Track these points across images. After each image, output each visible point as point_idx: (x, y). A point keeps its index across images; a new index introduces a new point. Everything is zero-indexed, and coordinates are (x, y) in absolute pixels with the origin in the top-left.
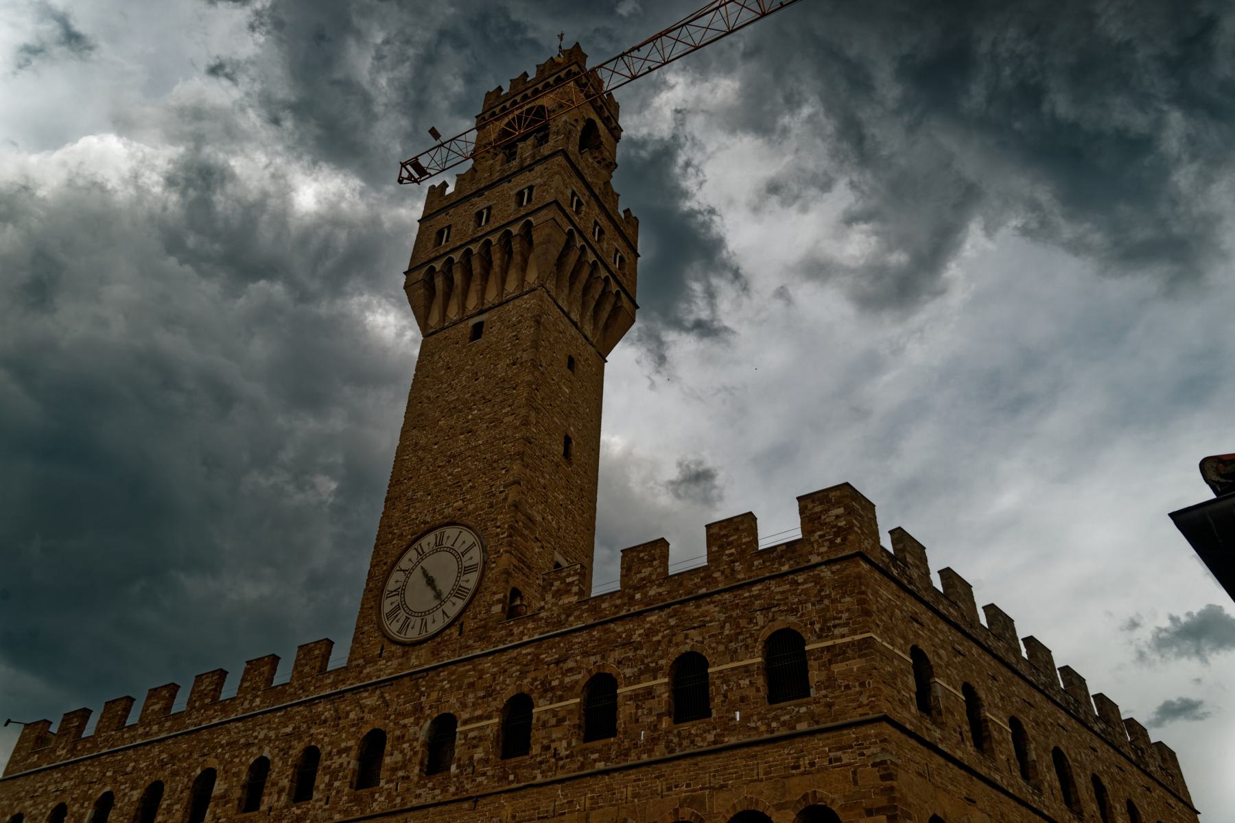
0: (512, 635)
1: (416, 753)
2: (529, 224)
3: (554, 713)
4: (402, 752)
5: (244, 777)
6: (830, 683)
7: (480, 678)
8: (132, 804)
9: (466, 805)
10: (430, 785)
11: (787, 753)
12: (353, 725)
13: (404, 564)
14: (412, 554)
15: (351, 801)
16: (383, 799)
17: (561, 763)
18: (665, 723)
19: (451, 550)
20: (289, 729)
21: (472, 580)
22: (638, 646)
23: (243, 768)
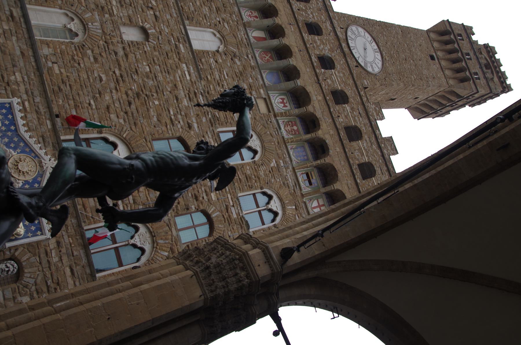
1: (321, 51)
2: (469, 80)
13: (367, 35)
14: (370, 38)
18: (357, 162)
21: (370, 69)
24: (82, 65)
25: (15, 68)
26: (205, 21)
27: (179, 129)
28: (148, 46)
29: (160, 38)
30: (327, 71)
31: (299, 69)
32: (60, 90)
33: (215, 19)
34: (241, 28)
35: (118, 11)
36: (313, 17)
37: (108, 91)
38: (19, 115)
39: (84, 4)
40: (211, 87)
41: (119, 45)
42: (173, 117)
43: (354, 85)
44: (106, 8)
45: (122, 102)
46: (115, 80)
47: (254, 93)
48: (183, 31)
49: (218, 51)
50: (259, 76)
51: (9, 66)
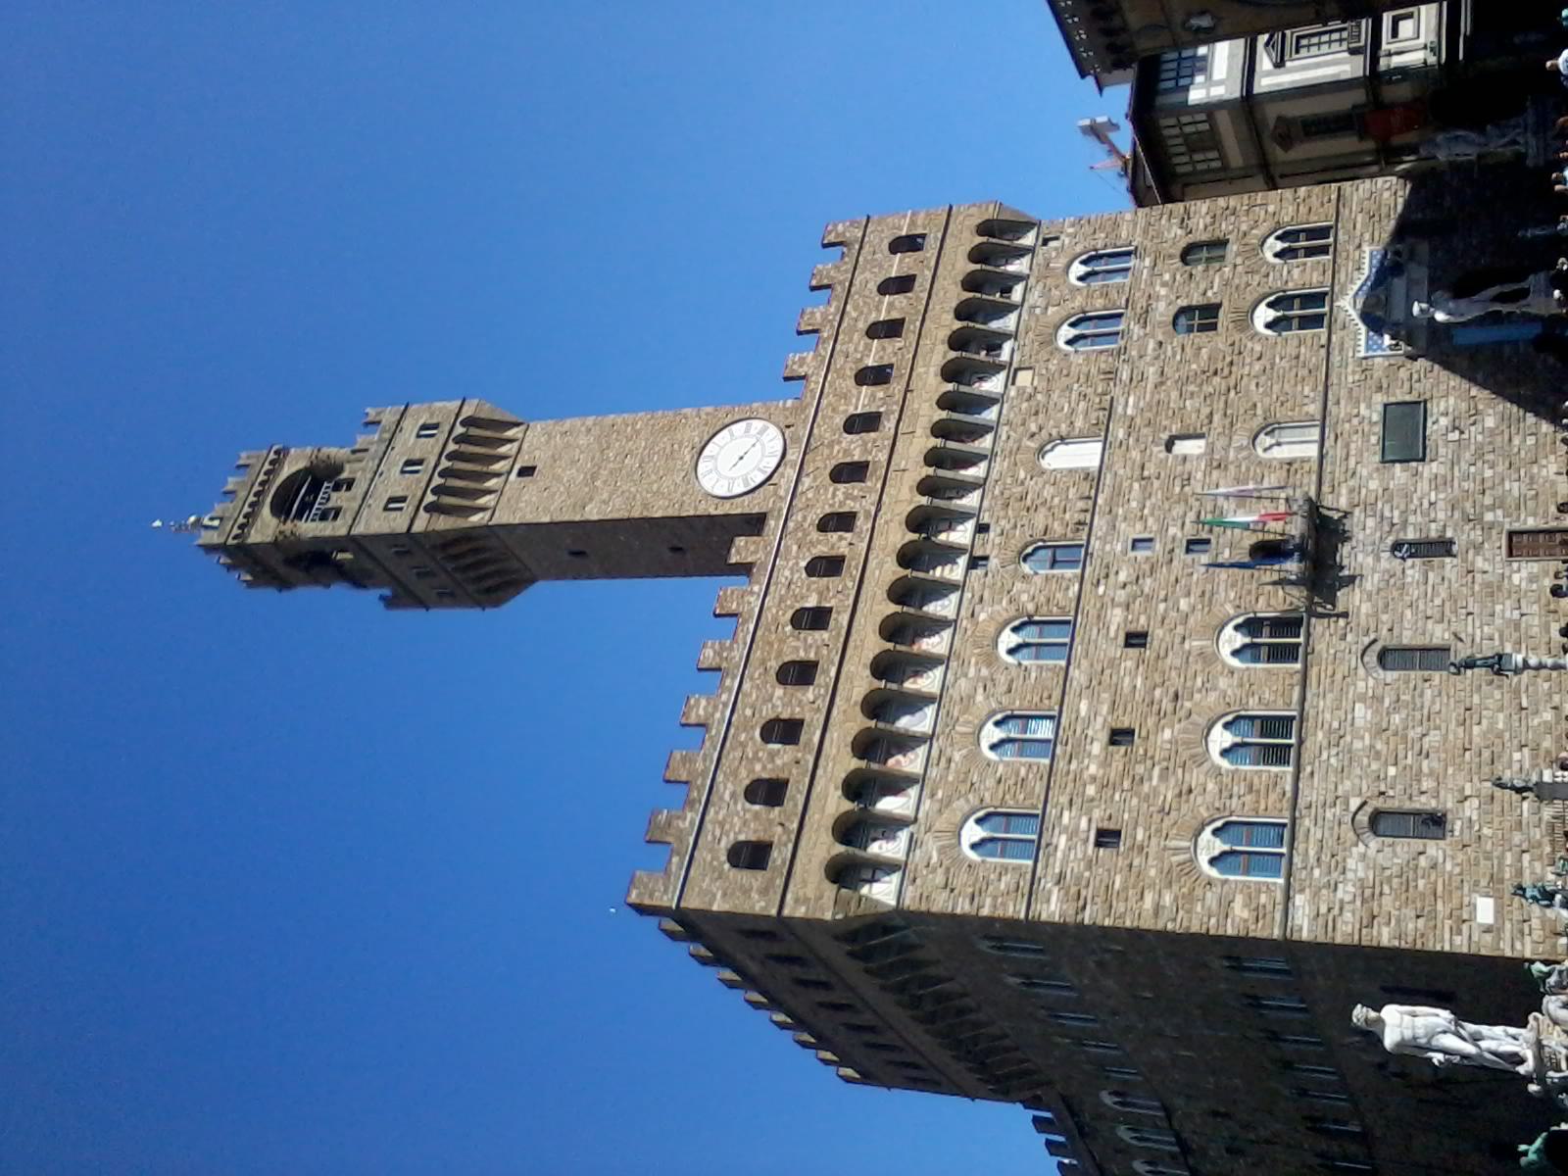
3: (877, 352)
8: (785, 694)
9: (909, 395)
18: (909, 295)
19: (722, 448)
21: (757, 424)
22: (862, 313)
24: (1275, 397)
25: (1350, 386)
26: (1059, 476)
28: (1174, 430)
30: (874, 410)
31: (935, 407)
32: (1310, 372)
33: (1036, 483)
34: (994, 475)
35: (1199, 465)
36: (836, 490)
37: (1252, 374)
38: (1363, 342)
42: (1179, 351)
43: (824, 396)
44: (1215, 464)
47: (1029, 390)
49: (1062, 439)
50: (1004, 412)
51: (1356, 389)
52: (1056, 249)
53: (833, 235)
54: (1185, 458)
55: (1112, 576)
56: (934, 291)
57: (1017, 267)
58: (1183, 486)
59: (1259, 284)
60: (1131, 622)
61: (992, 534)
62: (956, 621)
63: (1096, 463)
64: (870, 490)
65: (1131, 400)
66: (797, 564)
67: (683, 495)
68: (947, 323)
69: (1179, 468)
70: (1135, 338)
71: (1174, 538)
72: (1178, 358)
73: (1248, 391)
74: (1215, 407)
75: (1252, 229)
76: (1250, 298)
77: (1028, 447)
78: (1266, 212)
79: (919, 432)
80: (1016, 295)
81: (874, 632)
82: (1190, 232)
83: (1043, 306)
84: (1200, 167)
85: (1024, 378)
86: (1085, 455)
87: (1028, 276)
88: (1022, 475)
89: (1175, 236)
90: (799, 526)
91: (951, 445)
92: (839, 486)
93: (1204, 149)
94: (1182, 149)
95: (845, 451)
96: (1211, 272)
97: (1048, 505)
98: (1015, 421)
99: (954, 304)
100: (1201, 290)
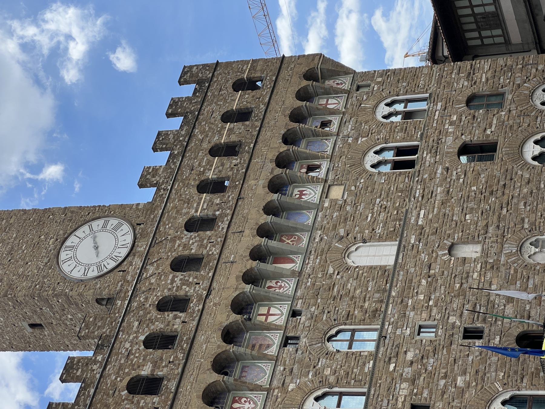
0: (162, 195)
1: (198, 236)
4: (193, 243)
5: (151, 350)
6: (262, 71)
7: (176, 208)
9: (240, 203)
10: (220, 224)
11: (281, 84)
12: (160, 278)
15: (206, 269)
16: (214, 249)
17: (242, 162)
18: (247, 123)
20: (136, 324)
21: (113, 222)
23: (144, 353)
24: (539, 214)
26: (361, 272)
27: (461, 168)
29: (437, 245)
30: (210, 213)
31: (262, 212)
33: (342, 277)
34: (308, 270)
39: (513, 268)
40: (397, 205)
41: (490, 235)
42: (463, 176)
44: (488, 267)
45: (512, 187)
46: (510, 204)
48: (401, 257)
49: (364, 241)
50: (319, 219)
52: (367, 93)
53: (189, 74)
54: (465, 258)
55: (401, 356)
56: (266, 121)
57: (333, 103)
58: (462, 283)
59: (529, 125)
60: (416, 395)
61: (303, 318)
62: (268, 390)
63: (391, 262)
64: (203, 278)
65: (422, 212)
66: (137, 337)
67: (44, 277)
68: (276, 146)
69: (459, 268)
70: (427, 164)
71: (453, 325)
72: (461, 180)
73: (517, 209)
74: (490, 222)
75: (525, 82)
76: (521, 137)
77: (338, 247)
78: (537, 69)
79: (247, 232)
80: (334, 128)
81: (198, 397)
82: (475, 83)
83: (355, 136)
84: (486, 41)
85: (337, 192)
86: (383, 254)
87: (344, 113)
88: (331, 270)
89: (463, 86)
90: (141, 306)
91: (273, 244)
92: (178, 273)
93: (491, 29)
94: (474, 26)
95: (186, 246)
96: (490, 115)
97: (351, 295)
98: (327, 226)
99: (283, 132)
100: (481, 129)
